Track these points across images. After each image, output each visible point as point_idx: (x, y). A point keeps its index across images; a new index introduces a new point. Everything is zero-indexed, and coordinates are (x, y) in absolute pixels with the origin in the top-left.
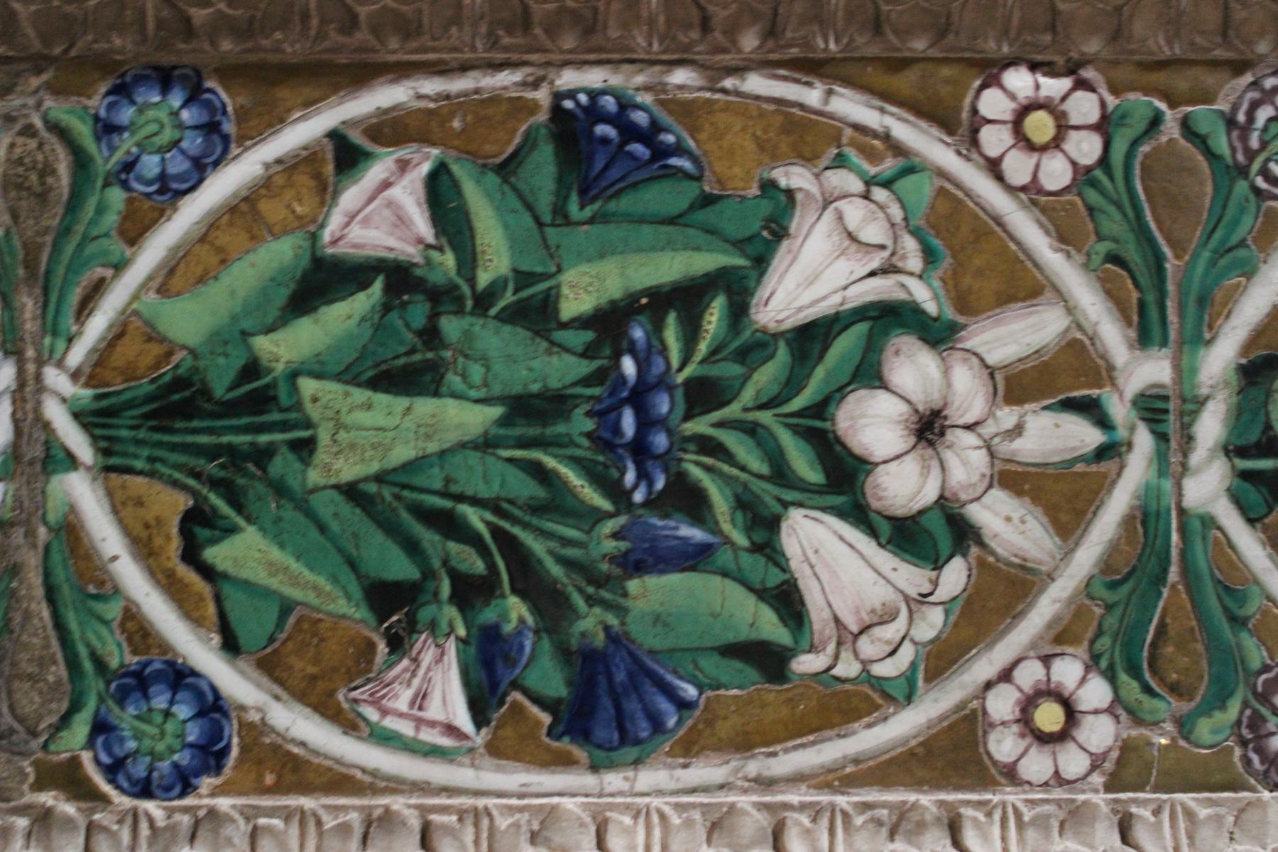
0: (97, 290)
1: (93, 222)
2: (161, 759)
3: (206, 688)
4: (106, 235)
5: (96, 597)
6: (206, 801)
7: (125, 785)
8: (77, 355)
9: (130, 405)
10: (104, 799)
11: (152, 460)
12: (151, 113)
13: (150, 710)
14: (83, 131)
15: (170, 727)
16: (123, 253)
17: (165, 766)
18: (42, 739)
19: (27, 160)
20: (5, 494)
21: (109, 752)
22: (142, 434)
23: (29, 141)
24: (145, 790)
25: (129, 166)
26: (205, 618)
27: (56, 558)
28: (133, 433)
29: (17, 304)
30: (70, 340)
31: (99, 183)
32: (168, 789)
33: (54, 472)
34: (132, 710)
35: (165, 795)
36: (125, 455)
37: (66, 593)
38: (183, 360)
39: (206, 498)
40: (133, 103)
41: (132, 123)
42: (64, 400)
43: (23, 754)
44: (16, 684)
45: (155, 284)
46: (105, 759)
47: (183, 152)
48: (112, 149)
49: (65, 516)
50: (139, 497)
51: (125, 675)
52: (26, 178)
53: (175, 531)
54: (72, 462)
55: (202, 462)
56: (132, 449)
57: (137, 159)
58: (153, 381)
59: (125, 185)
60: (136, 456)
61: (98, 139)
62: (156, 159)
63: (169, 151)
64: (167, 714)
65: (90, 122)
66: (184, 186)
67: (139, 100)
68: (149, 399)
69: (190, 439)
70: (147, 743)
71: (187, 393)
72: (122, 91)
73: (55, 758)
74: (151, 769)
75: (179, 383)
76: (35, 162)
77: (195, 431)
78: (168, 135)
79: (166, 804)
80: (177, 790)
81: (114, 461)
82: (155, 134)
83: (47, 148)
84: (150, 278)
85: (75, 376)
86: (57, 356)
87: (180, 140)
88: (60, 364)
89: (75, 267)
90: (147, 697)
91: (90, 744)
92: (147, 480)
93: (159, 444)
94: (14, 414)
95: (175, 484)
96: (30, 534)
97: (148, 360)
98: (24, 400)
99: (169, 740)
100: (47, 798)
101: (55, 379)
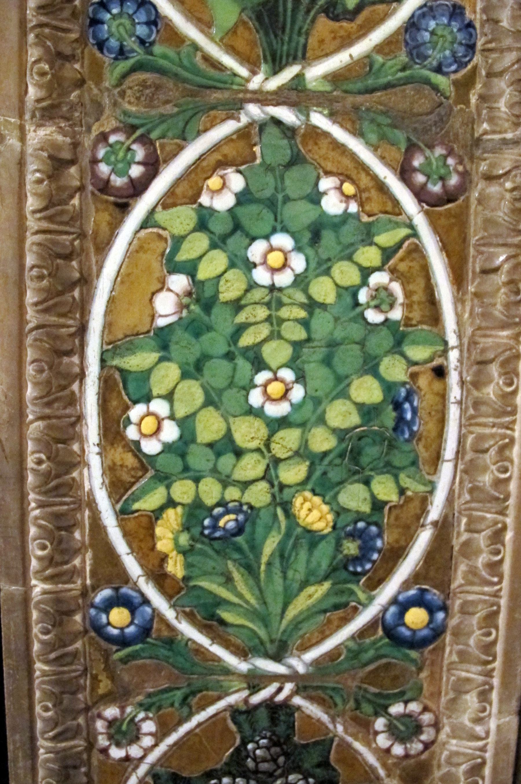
0: (207, 59)
1: (172, 61)
2: (456, 38)
3: (420, 12)
4: (179, 54)
5: (371, 66)
6: (478, 16)
7: (467, 59)
8: (243, 72)
9: (270, 44)
10: (475, 69)
11: (299, 34)
12: (114, 29)
13: (430, 42)
14: (123, 66)
15: (439, 33)
16: (188, 45)
17: (460, 36)
18: (444, 100)
19: (138, 95)
20: (315, 111)
21: (450, 65)
22: (286, 38)
23: (127, 94)
24: (471, 47)
25: (142, 42)
26: (383, 11)
27: (350, 87)
28: (286, 44)
29: (215, 101)
30: (235, 75)
31: (150, 57)
32: (471, 35)
33: (305, 86)
34: (430, 52)
35: (474, 36)
36: (296, 50)
37: (370, 82)
38: (247, 16)
39: (321, 7)
40: (107, 39)
41: (118, 40)
42: (266, 79)
43: (451, 109)
44: (415, 111)
45: (206, 29)
46: (454, 68)
47: (135, 12)
48: (133, 51)
49: (329, 81)
50: (319, 42)
51: (412, 55)
52: (147, 95)
53: (337, 24)
54: (299, 77)
55: (302, 7)
56: (293, 44)
57: (138, 37)
58: (257, 31)
59: (152, 44)
60: (298, 43)
61: (127, 58)
62: (138, 27)
63: (134, 20)
64: (433, 33)
65: (117, 63)
66: (153, 12)
67: (106, 36)
68: (267, 34)
69: (289, 13)
70: (447, 45)
71: (265, 14)
72: (101, 45)
73: (453, 94)
74: (461, 44)
75: (259, 18)
76: (139, 91)
77: (285, 11)
78: (126, 21)
79: (479, 36)
80: (471, 30)
81: (300, 54)
82: (125, 27)
83: (131, 85)
84: (202, 31)
85: (254, 73)
86: (243, 82)
87: (128, 14)
88: (248, 80)
89: (196, 71)
90: (424, 43)
91: (446, 74)
92: (310, 37)
93: (292, 29)
94: (275, 105)
95: (313, 21)
96: (336, 100)
97: (246, 34)
98: (266, 100)
99: (446, 33)
100: (473, 99)
101: (255, 83)
